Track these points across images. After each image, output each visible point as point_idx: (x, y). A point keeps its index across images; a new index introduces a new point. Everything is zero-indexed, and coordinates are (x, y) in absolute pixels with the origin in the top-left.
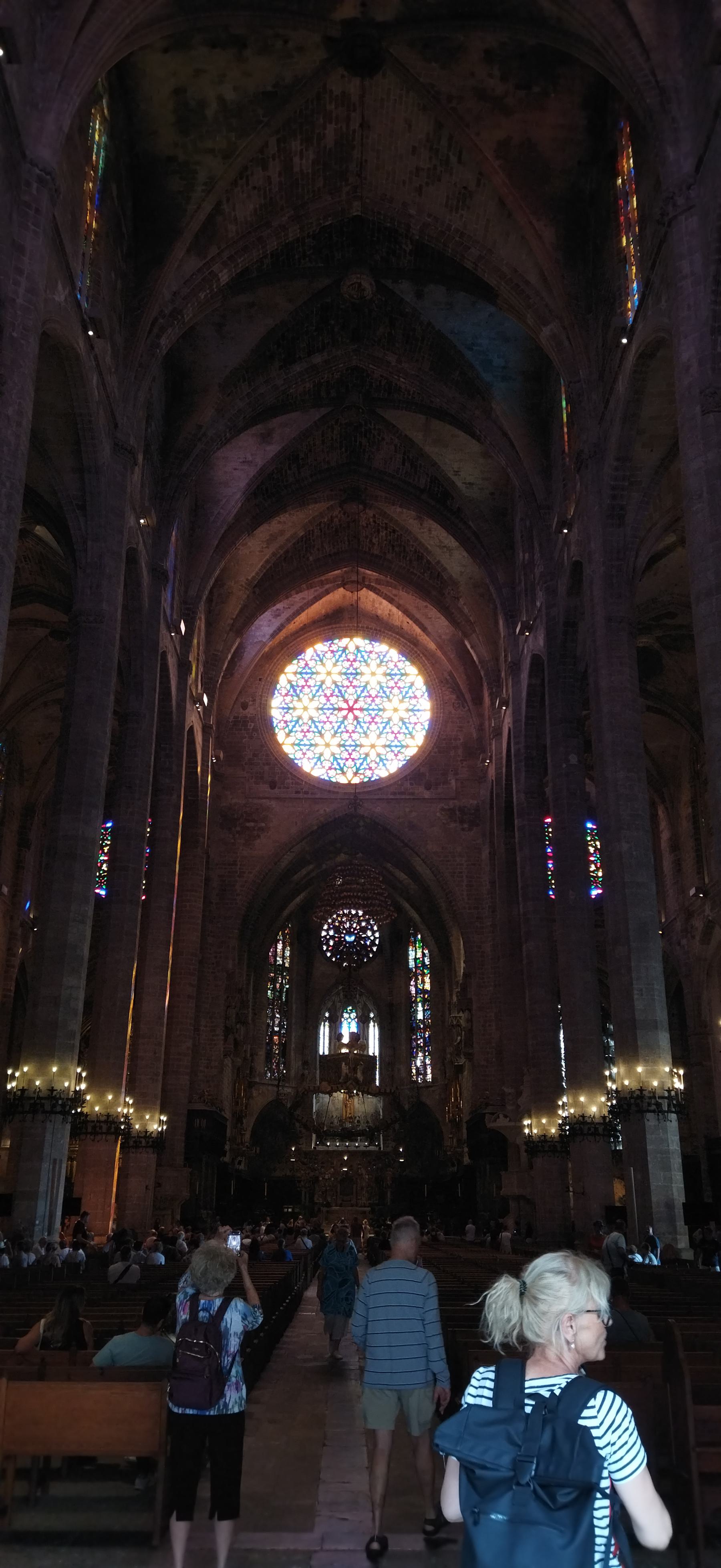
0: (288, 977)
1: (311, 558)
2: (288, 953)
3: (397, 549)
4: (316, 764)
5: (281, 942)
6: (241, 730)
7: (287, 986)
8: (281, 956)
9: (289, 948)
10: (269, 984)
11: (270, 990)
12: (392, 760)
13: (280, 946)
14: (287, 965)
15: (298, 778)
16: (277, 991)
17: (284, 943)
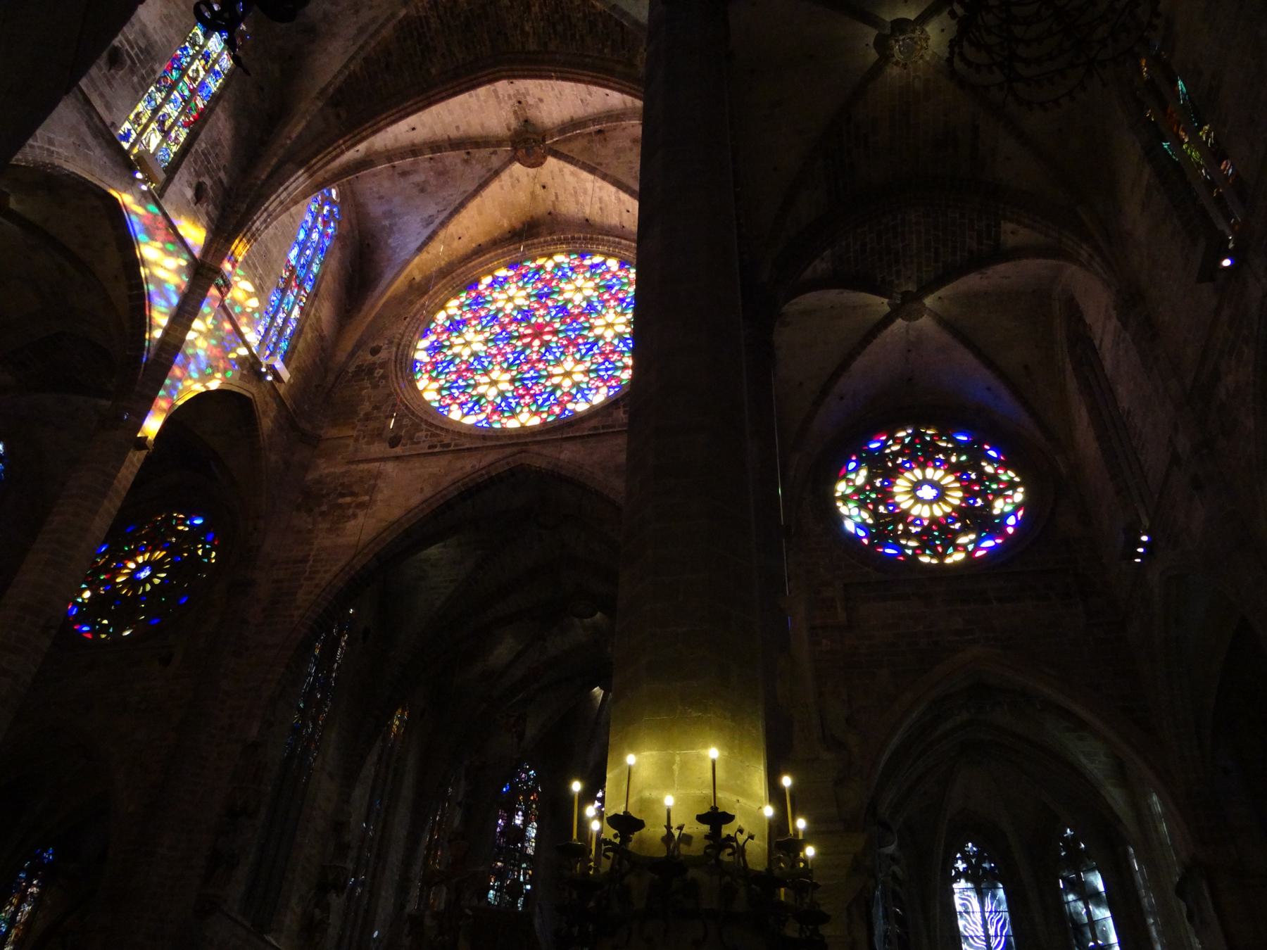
1: (433, 71)
3: (560, 28)
4: (472, 409)
5: (520, 813)
6: (364, 379)
10: (493, 880)
11: (493, 889)
12: (598, 388)
15: (437, 427)
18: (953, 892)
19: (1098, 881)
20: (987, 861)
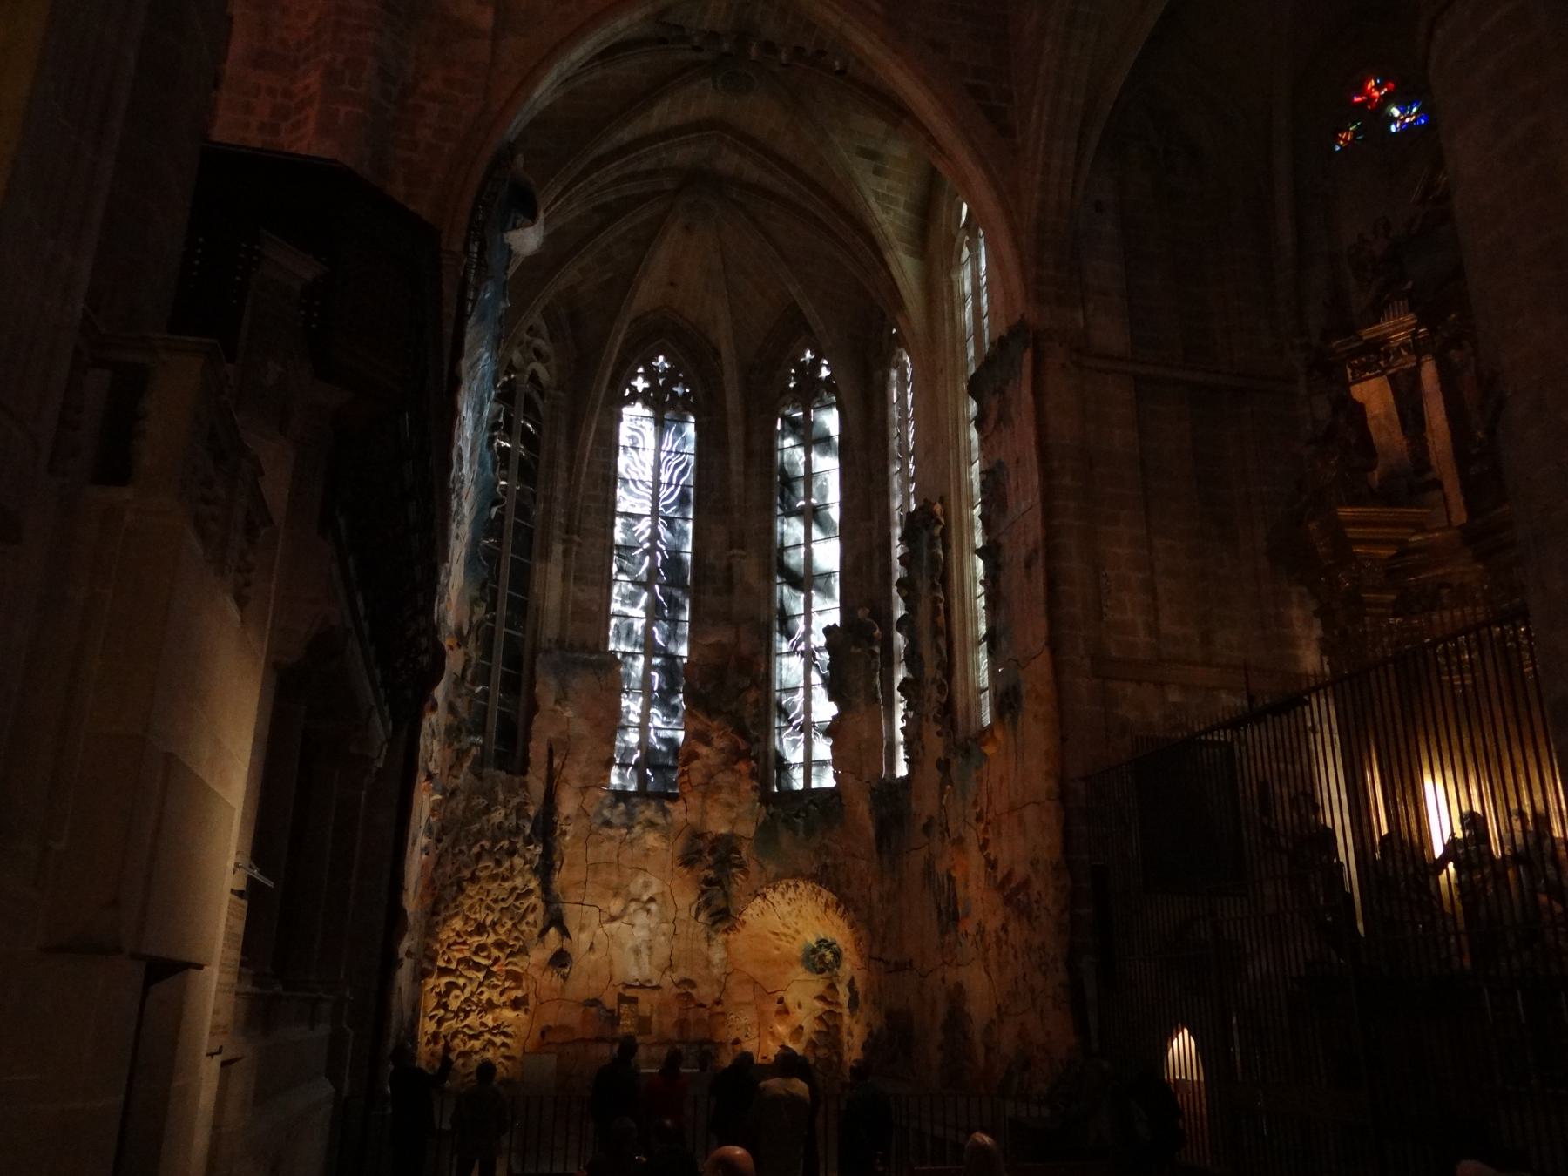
18: (620, 419)
19: (830, 420)
20: (680, 384)
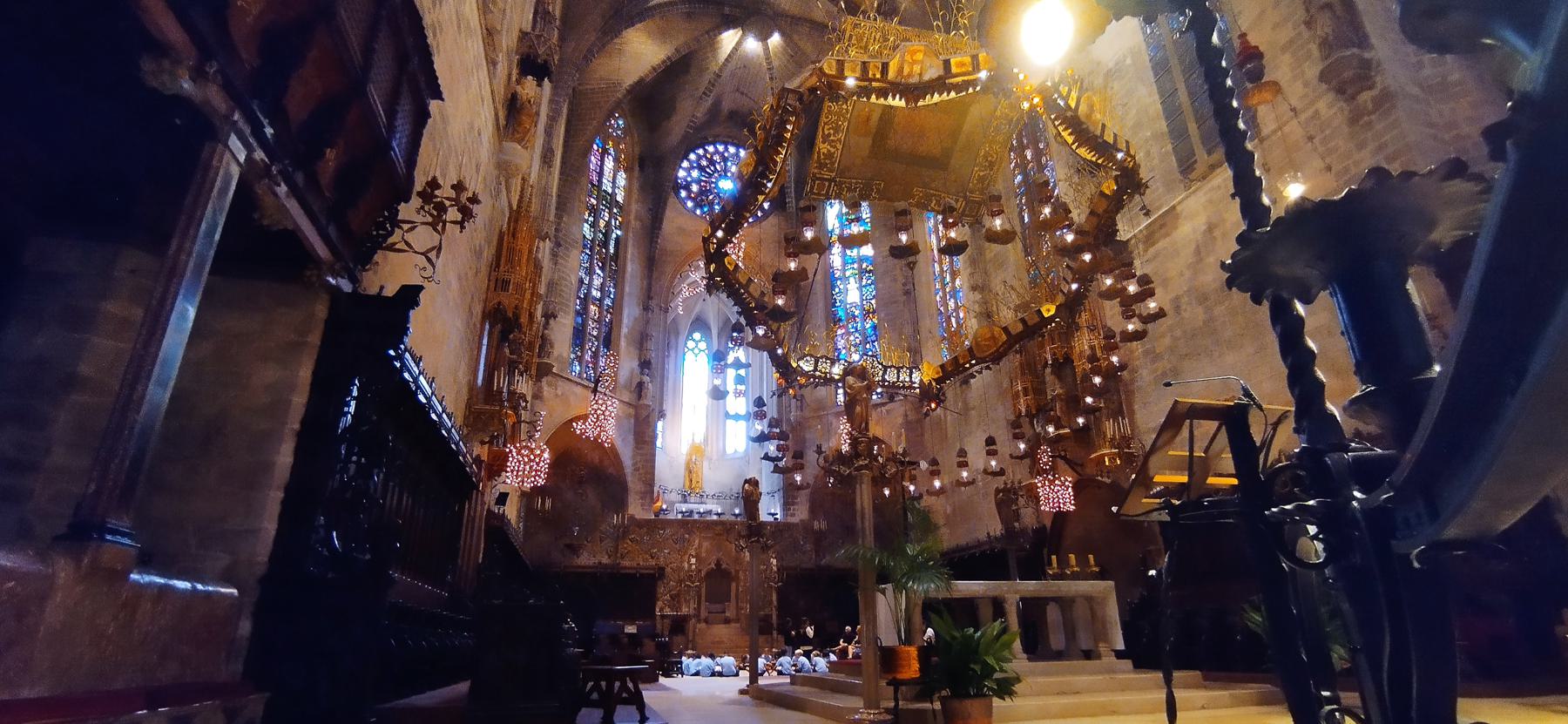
0: (620, 219)
2: (622, 179)
7: (619, 233)
8: (611, 180)
9: (624, 176)
13: (609, 164)
14: (620, 198)
16: (600, 231)
17: (616, 160)
